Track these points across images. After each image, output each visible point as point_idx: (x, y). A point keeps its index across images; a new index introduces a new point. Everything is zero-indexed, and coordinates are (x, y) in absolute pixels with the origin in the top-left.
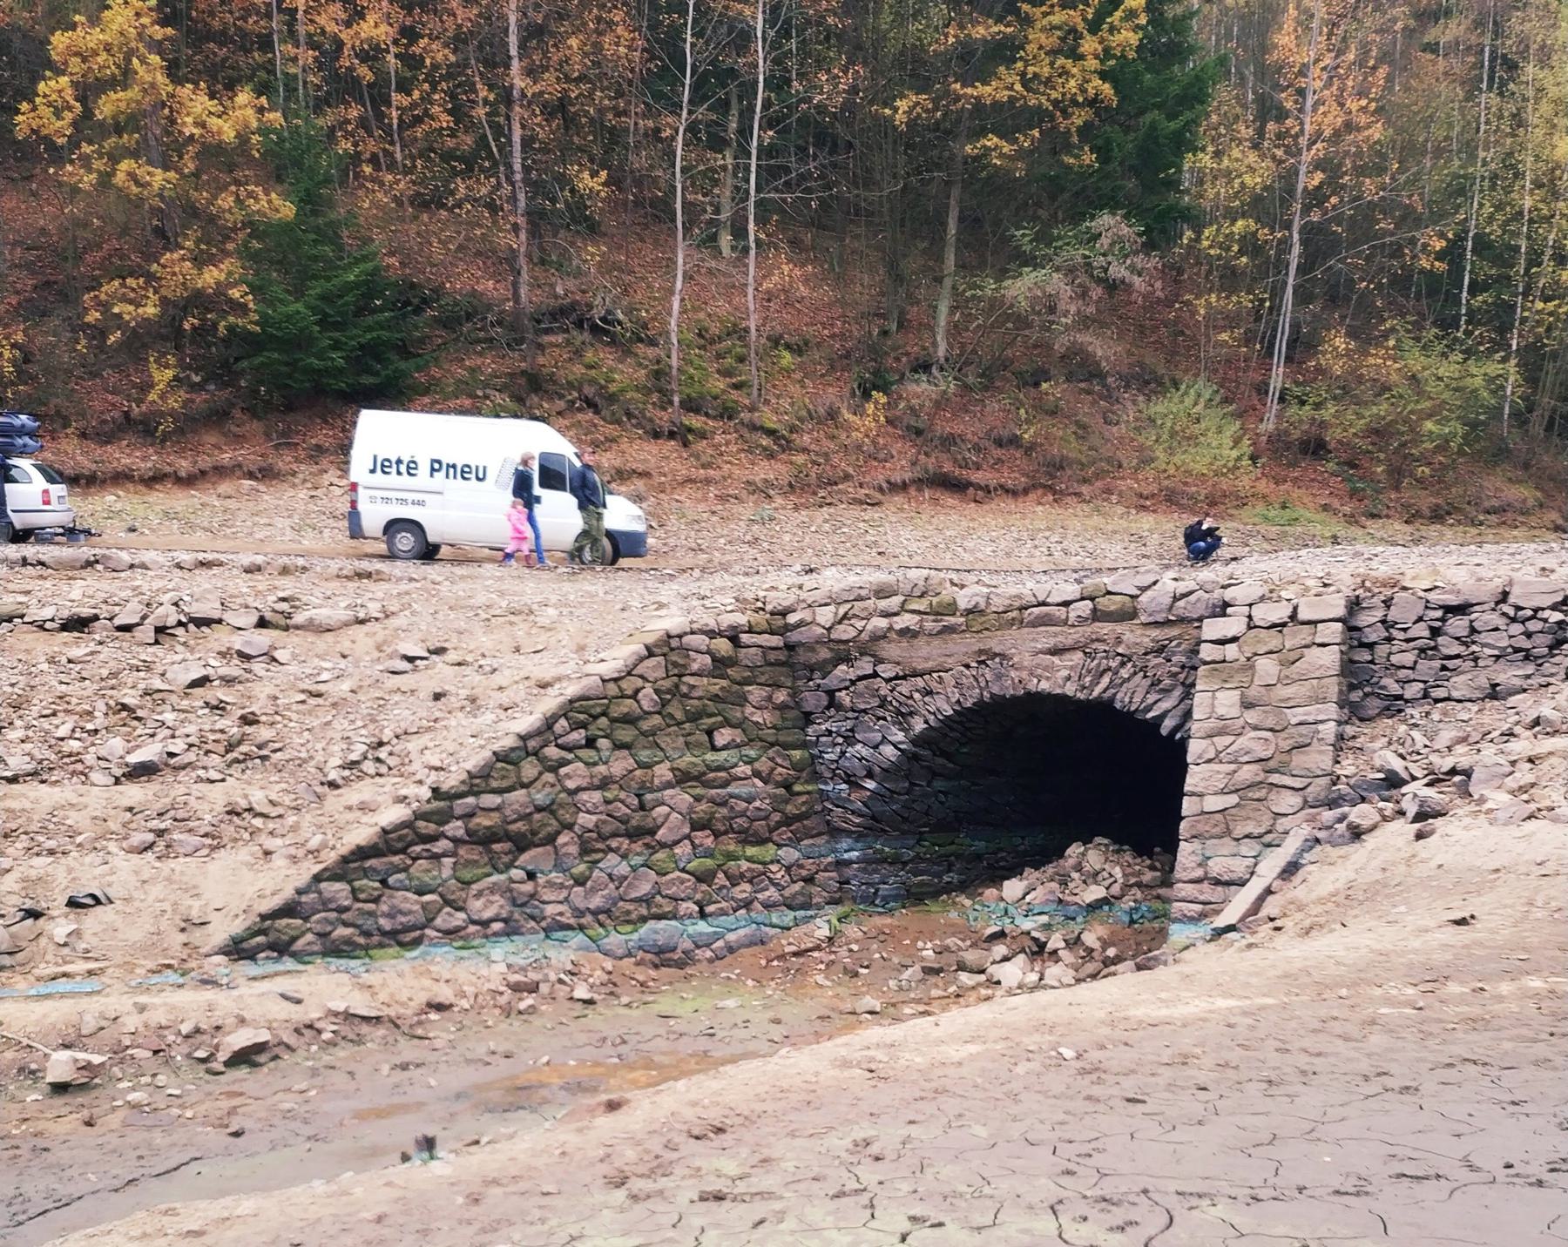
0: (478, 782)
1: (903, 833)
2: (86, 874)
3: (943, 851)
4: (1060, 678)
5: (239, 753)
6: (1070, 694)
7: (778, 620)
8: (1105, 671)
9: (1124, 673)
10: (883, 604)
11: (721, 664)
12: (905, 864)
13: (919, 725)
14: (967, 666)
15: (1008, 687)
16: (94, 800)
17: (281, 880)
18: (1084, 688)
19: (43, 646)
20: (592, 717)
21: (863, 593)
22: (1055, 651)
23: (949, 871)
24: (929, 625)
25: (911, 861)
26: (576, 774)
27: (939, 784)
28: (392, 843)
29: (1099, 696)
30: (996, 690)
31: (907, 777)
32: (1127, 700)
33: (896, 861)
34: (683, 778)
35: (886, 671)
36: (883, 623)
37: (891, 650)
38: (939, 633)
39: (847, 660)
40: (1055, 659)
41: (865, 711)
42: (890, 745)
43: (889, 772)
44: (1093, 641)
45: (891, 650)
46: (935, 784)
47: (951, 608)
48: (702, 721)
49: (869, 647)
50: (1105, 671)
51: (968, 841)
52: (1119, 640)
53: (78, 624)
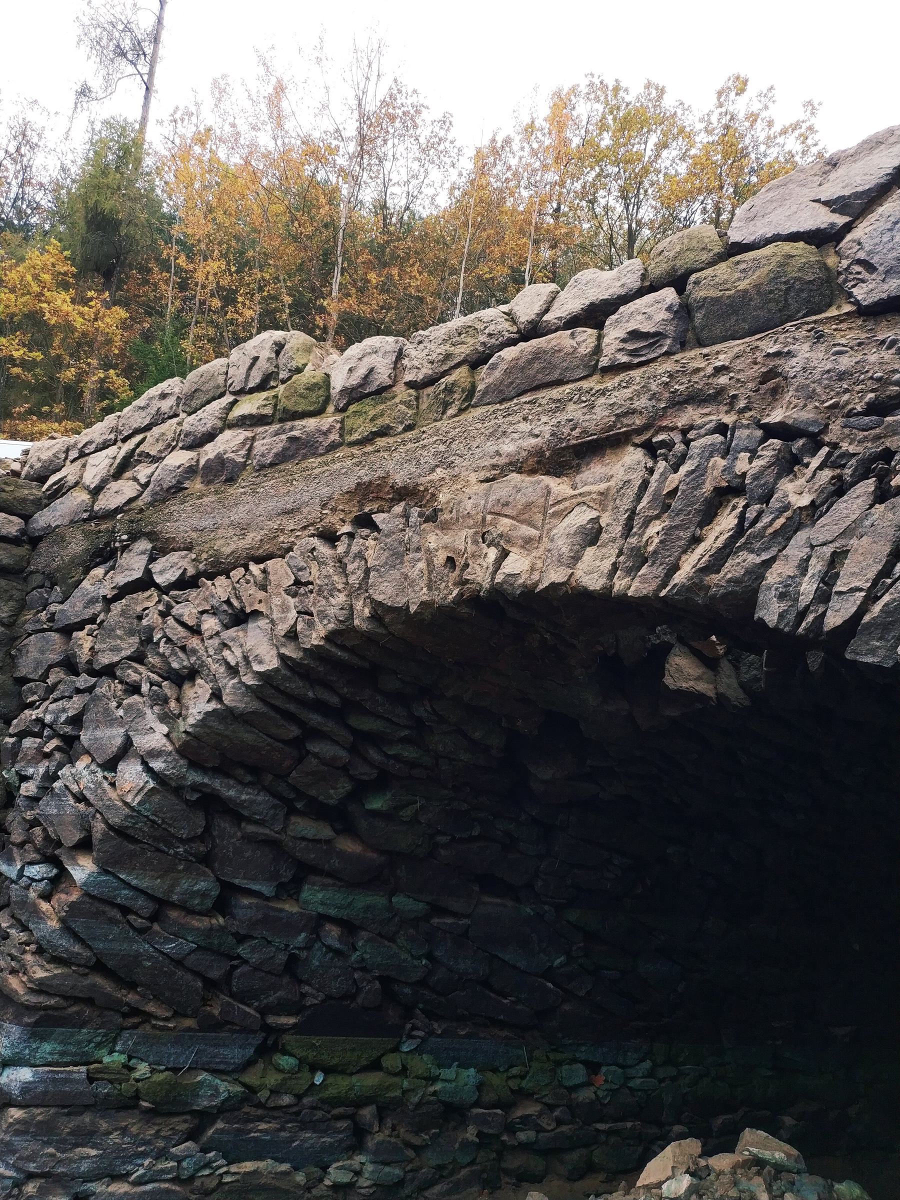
1: (210, 1025)
3: (341, 1085)
4: (562, 540)
6: (594, 582)
8: (723, 495)
9: (796, 492)
10: (190, 423)
12: (206, 1117)
13: (198, 703)
14: (330, 537)
15: (408, 575)
18: (640, 558)
21: (166, 405)
22: (564, 457)
23: (357, 1139)
24: (269, 442)
25: (226, 1109)
27: (316, 896)
29: (696, 585)
30: (385, 591)
31: (206, 860)
32: (808, 587)
33: (167, 1105)
35: (166, 571)
36: (180, 458)
37: (181, 521)
38: (282, 458)
39: (105, 555)
40: (559, 487)
41: (109, 671)
43: (125, 840)
44: (679, 402)
45: (181, 521)
46: (306, 894)
47: (320, 398)
50: (723, 495)
51: (423, 1064)
52: (772, 382)
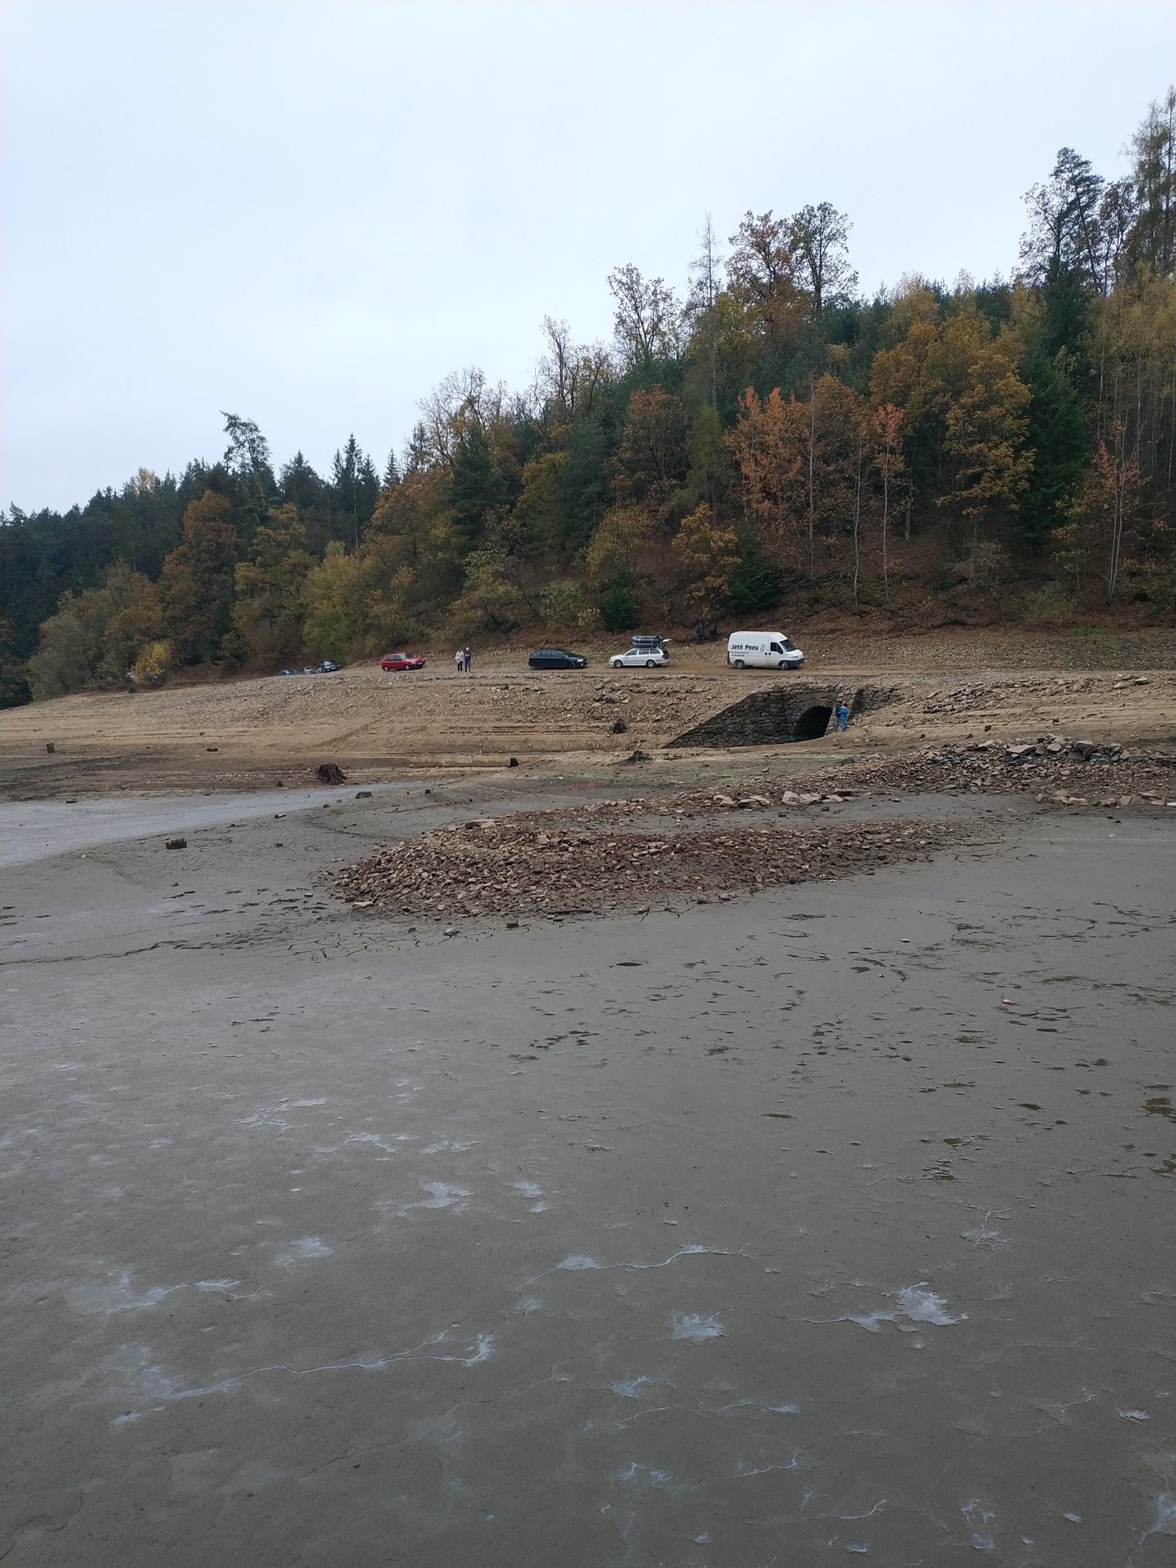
0: (708, 723)
2: (644, 737)
5: (673, 718)
7: (781, 690)
11: (765, 700)
16: (650, 725)
17: (673, 738)
19: (648, 697)
20: (733, 711)
26: (728, 721)
28: (690, 733)
34: (752, 723)
42: (797, 716)
43: (798, 722)
48: (758, 711)
49: (795, 696)
53: (654, 693)
